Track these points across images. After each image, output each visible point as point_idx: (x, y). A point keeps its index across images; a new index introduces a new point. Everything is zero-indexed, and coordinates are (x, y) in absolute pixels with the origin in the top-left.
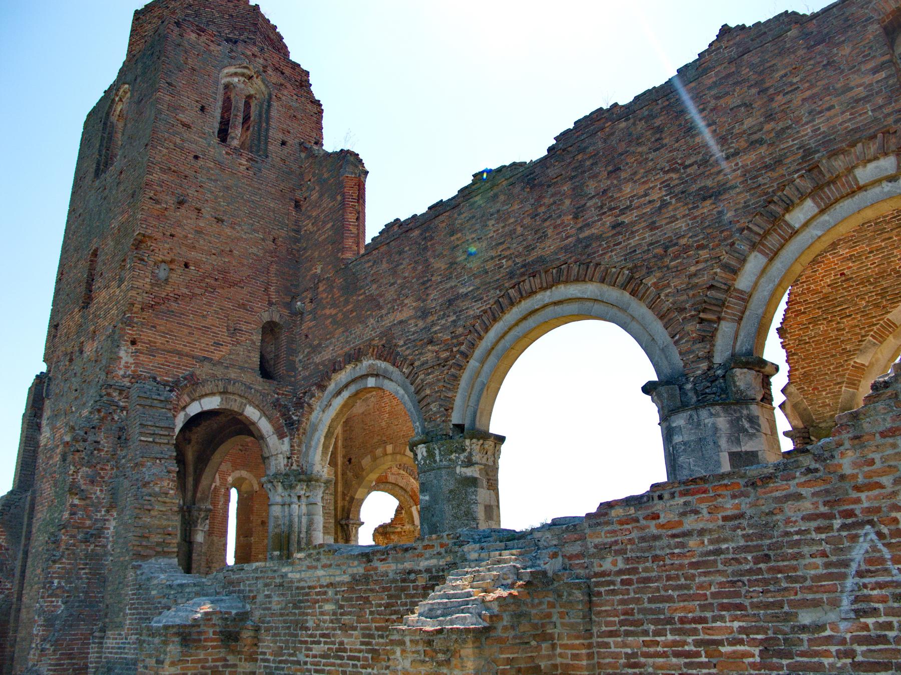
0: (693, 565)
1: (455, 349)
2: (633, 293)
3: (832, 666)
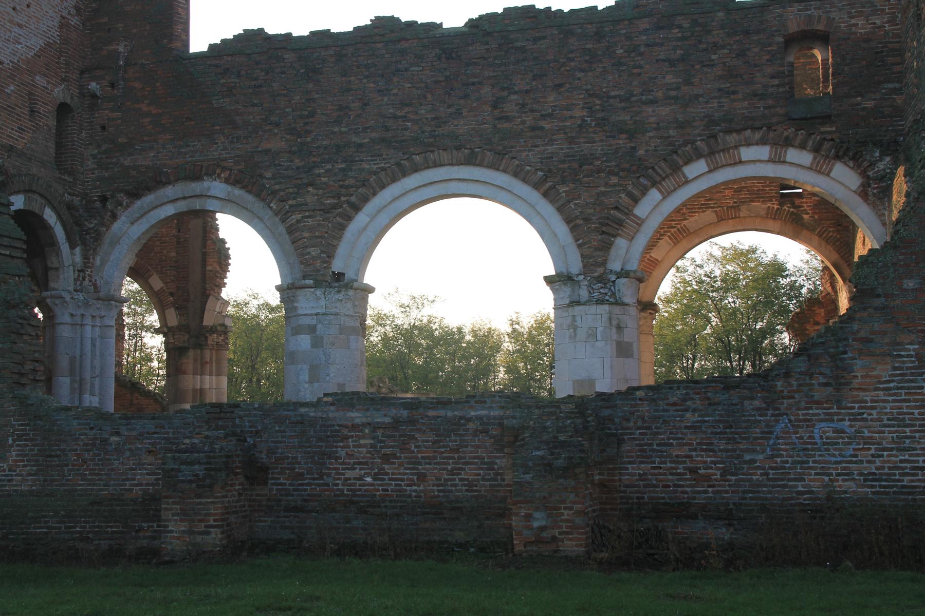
0: (686, 427)
1: (343, 199)
2: (545, 195)
3: (757, 480)
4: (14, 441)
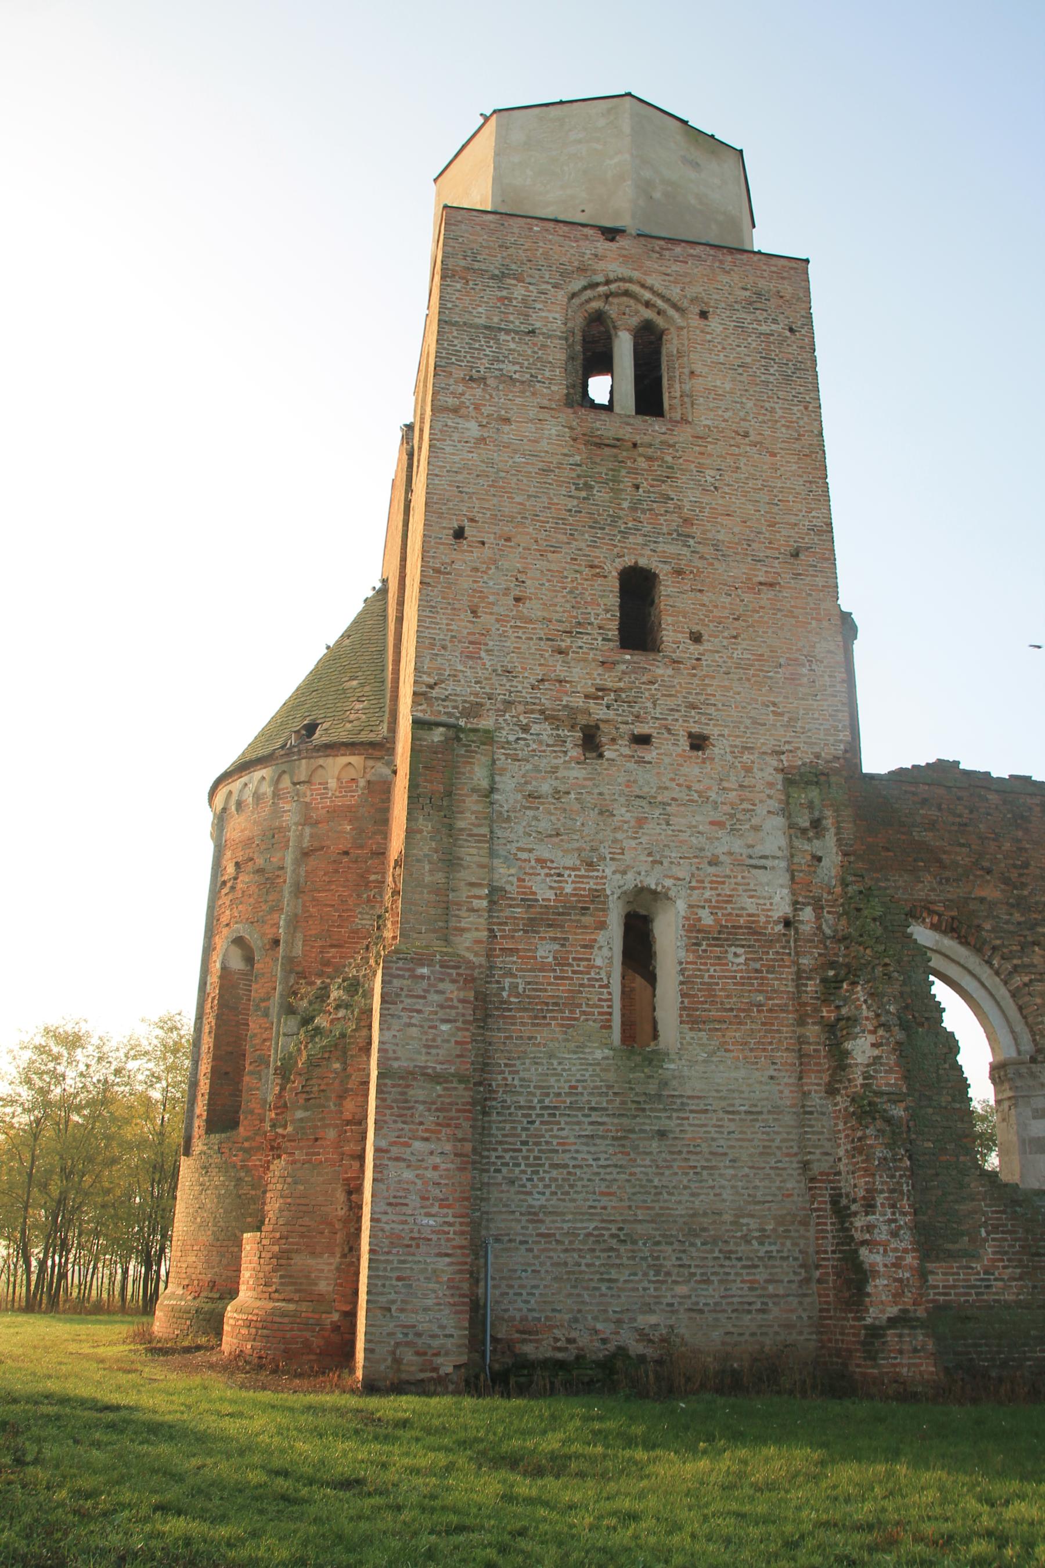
4: (988, 1233)
